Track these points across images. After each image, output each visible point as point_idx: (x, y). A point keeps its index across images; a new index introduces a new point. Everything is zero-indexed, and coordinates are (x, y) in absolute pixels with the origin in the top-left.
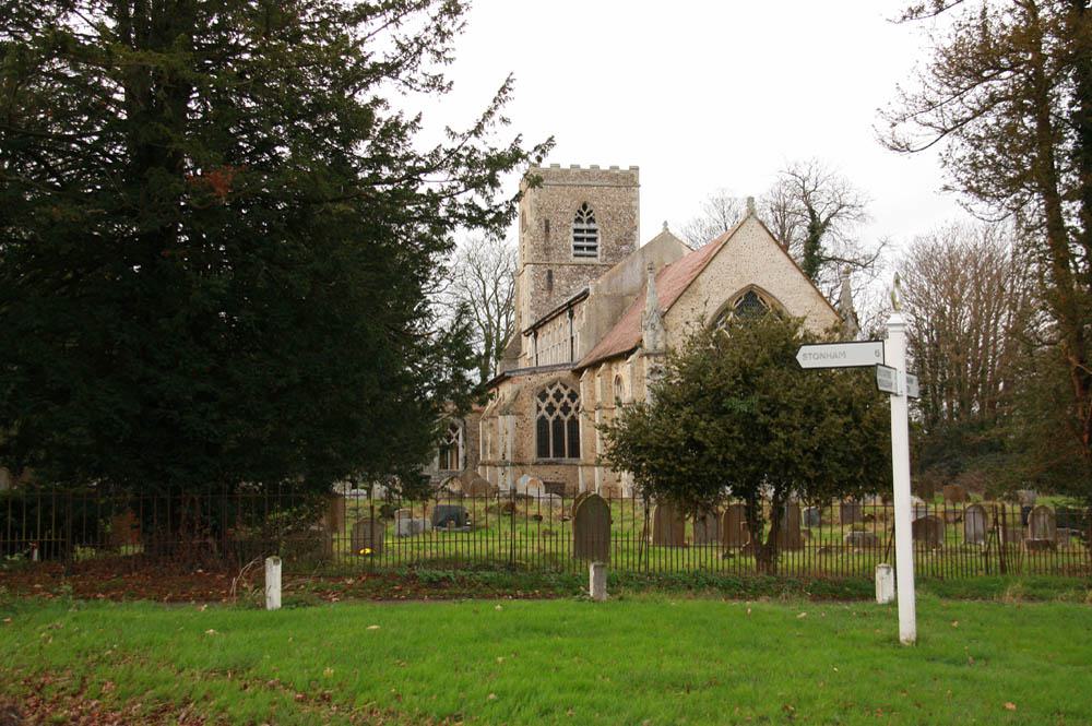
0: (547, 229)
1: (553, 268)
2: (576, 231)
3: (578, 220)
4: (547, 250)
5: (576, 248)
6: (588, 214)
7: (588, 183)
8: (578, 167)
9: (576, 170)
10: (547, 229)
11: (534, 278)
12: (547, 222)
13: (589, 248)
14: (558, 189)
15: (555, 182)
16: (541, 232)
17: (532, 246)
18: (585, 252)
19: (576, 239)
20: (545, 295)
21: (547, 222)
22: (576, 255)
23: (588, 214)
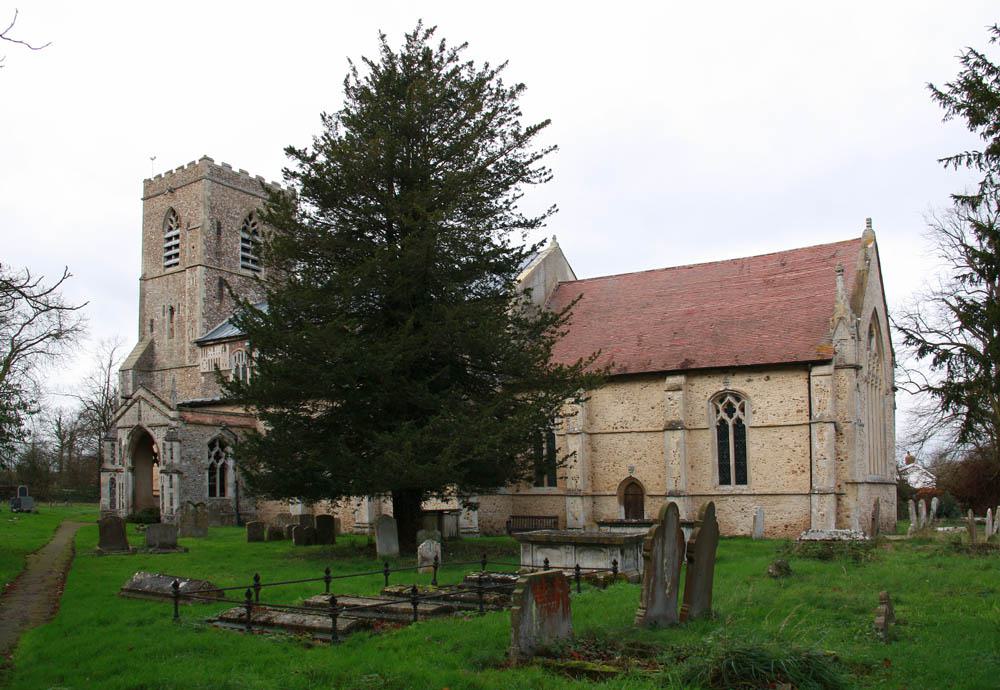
0: (219, 229)
1: (224, 276)
2: (244, 240)
3: (245, 229)
4: (219, 254)
5: (244, 259)
6: (253, 225)
7: (255, 192)
8: (247, 174)
9: (243, 176)
10: (219, 229)
11: (207, 282)
12: (219, 224)
13: (254, 261)
14: (230, 191)
15: (227, 184)
16: (212, 233)
17: (204, 247)
18: (250, 264)
19: (244, 249)
20: (217, 303)
21: (219, 224)
22: (243, 267)
23: (253, 225)
